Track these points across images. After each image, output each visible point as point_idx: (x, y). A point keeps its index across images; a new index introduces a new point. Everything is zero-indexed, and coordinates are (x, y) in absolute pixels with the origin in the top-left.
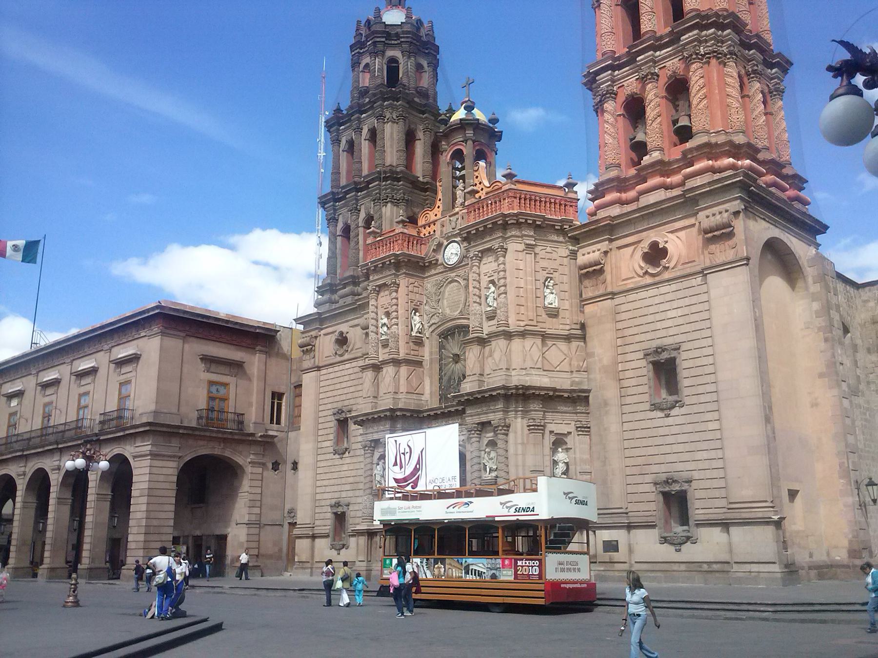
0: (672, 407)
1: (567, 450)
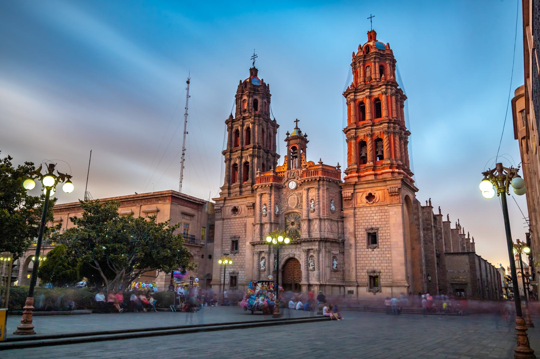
0: (375, 248)
1: (336, 260)
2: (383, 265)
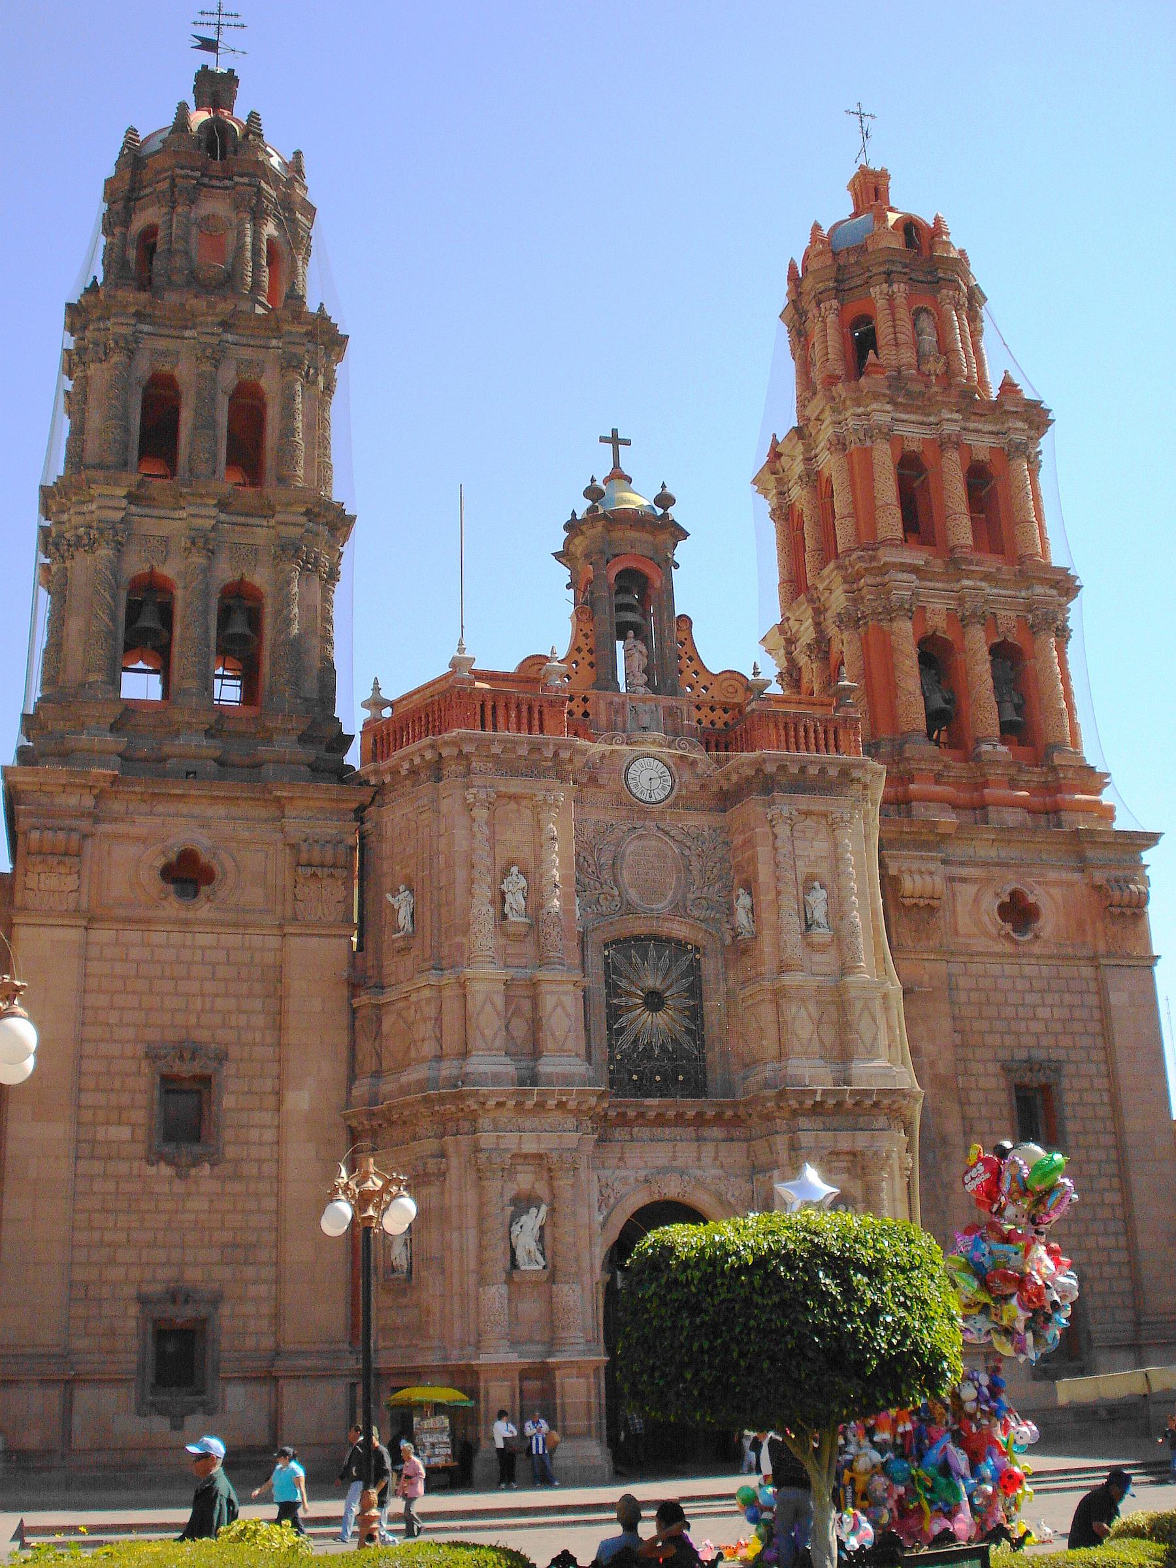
2: (1090, 1243)
